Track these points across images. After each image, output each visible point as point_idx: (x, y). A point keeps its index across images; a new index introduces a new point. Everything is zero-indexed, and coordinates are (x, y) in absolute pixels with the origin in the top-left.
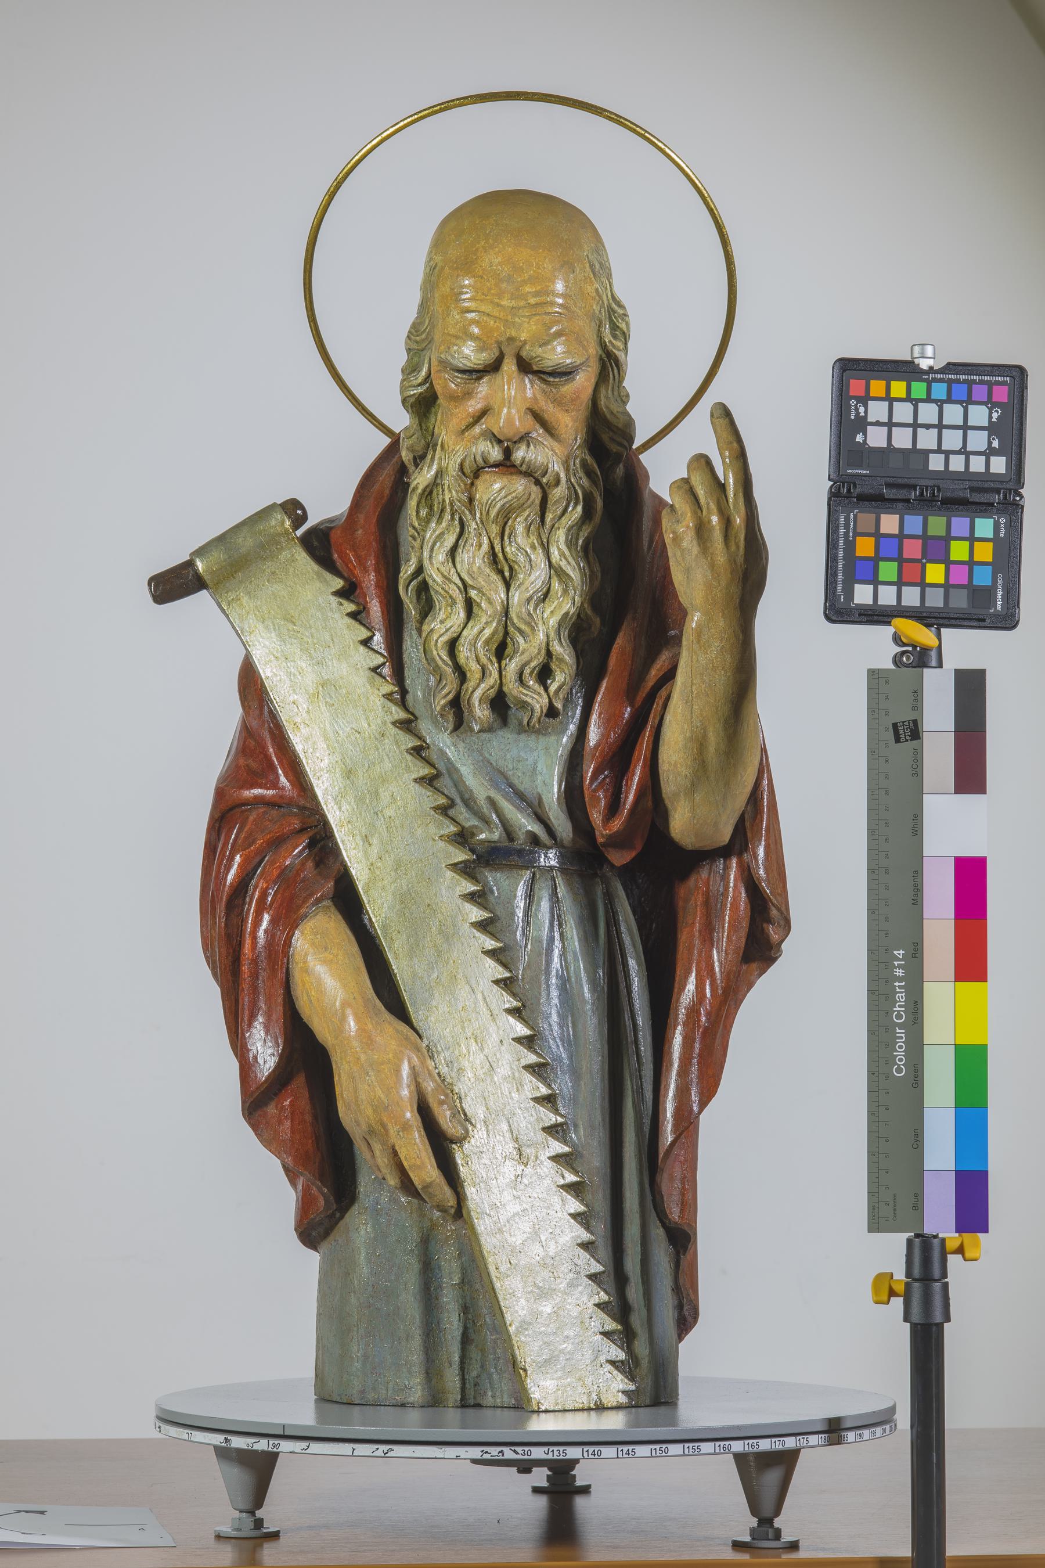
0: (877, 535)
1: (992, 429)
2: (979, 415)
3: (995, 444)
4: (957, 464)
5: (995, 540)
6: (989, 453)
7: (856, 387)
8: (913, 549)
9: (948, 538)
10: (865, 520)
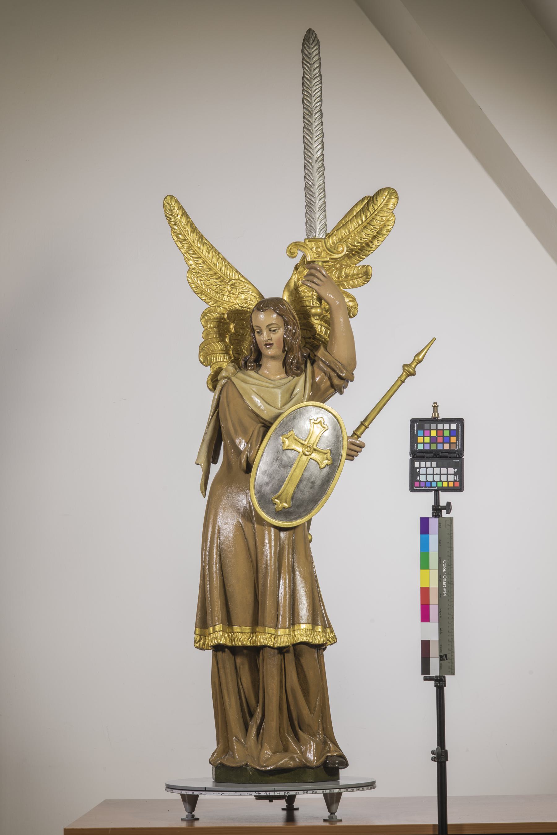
0: (450, 443)
1: (419, 474)
2: (423, 478)
3: (418, 470)
4: (428, 464)
5: (417, 443)
6: (419, 468)
7: (457, 485)
8: (440, 440)
9: (430, 443)
10: (453, 447)
